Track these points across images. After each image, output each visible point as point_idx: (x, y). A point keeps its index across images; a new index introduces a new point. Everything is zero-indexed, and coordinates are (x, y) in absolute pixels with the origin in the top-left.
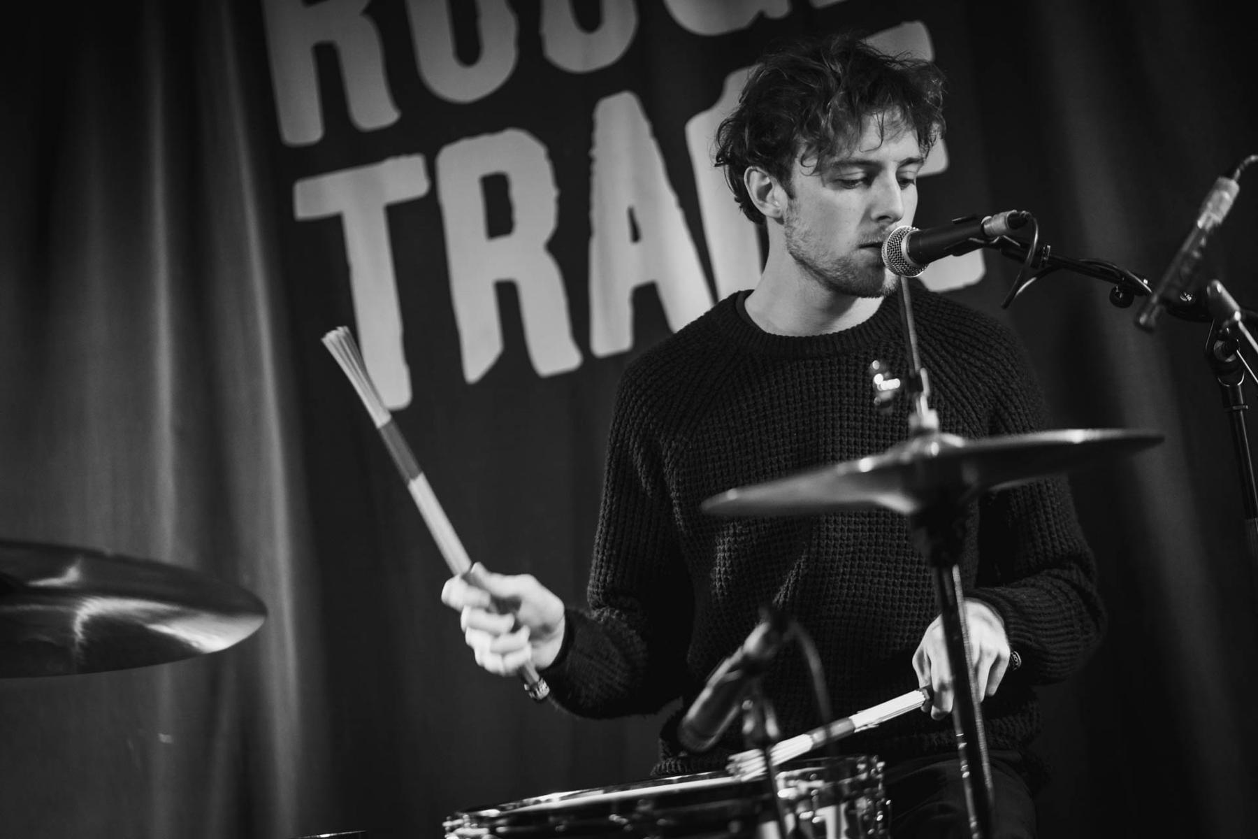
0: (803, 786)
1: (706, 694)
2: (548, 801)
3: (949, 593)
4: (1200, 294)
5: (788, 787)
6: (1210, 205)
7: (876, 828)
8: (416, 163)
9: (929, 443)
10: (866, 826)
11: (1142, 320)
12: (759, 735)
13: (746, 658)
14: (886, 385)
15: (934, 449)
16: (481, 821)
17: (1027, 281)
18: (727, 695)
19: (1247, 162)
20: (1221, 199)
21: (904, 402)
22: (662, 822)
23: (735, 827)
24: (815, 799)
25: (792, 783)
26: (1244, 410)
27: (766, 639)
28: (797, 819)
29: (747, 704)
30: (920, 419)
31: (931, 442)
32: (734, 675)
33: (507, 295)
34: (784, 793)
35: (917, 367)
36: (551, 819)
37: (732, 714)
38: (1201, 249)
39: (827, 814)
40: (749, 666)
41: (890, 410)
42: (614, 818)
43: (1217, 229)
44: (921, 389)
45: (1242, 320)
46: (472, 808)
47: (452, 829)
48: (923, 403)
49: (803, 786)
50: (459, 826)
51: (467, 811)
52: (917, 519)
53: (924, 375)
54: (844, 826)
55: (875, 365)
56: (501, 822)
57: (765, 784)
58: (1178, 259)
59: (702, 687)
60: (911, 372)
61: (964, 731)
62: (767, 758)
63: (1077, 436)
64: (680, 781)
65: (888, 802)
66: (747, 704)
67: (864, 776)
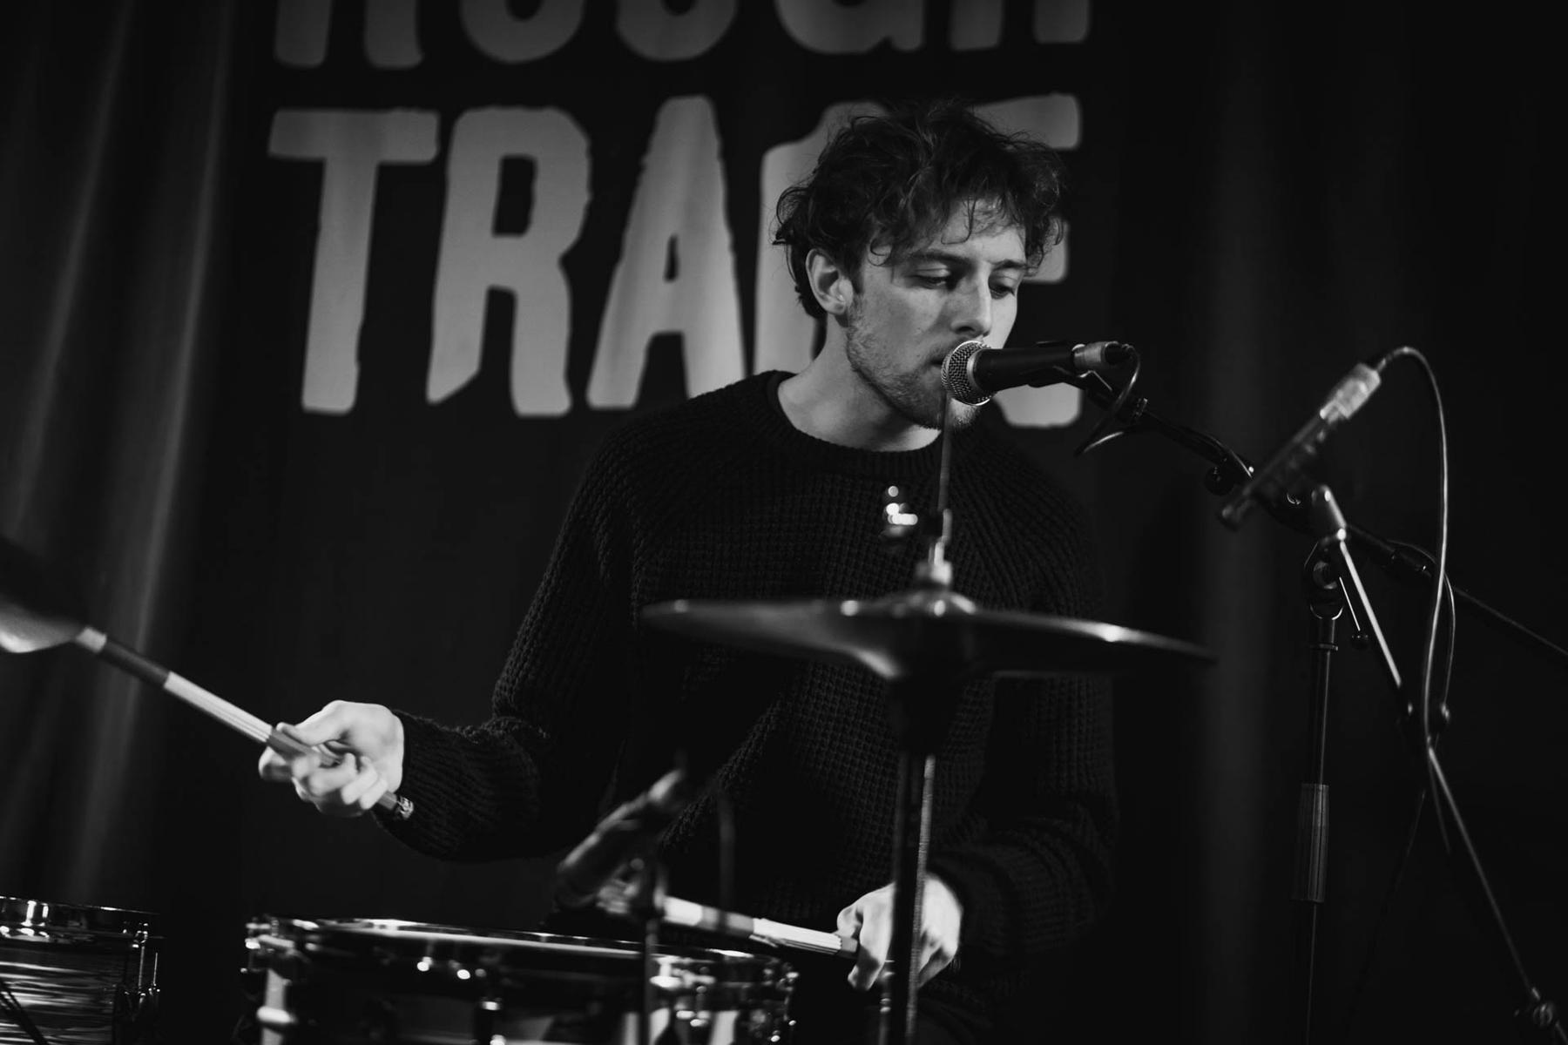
0: (690, 978)
1: (592, 840)
2: (383, 927)
3: (915, 790)
5: (673, 976)
6: (1340, 394)
8: (428, 123)
11: (1226, 512)
14: (899, 517)
15: (939, 608)
16: (288, 931)
17: (1110, 434)
19: (1397, 352)
20: (1355, 391)
21: (916, 543)
22: (507, 982)
24: (700, 998)
25: (677, 971)
26: (1333, 651)
27: (676, 792)
28: (673, 1017)
29: (637, 863)
30: (930, 569)
31: (938, 599)
32: (629, 825)
33: (501, 308)
34: (665, 979)
35: (941, 505)
38: (1317, 444)
40: (651, 817)
43: (1342, 423)
44: (939, 533)
45: (1346, 541)
46: (284, 916)
47: (256, 934)
48: (938, 551)
49: (690, 978)
51: (278, 916)
53: (947, 518)
55: (892, 491)
56: (313, 937)
64: (550, 940)
65: (792, 1023)
66: (637, 863)
67: (768, 983)
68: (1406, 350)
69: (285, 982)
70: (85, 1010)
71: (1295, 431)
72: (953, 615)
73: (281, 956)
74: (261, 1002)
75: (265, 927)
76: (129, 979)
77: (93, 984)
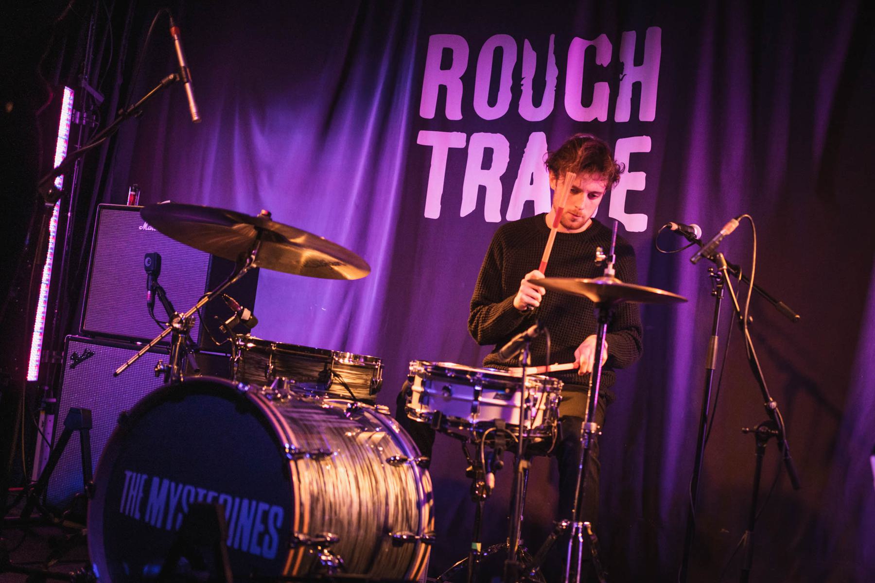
0: (534, 383)
1: (510, 344)
3: (601, 333)
4: (715, 256)
5: (529, 382)
7: (554, 404)
9: (608, 280)
10: (551, 402)
12: (524, 362)
13: (527, 335)
14: (600, 256)
15: (610, 282)
16: (423, 365)
18: (517, 346)
20: (731, 226)
21: (604, 264)
22: (483, 382)
23: (507, 391)
24: (537, 389)
25: (531, 381)
27: (535, 330)
28: (529, 394)
29: (523, 351)
36: (447, 371)
37: (518, 352)
38: (719, 241)
39: (539, 395)
40: (527, 338)
41: (599, 265)
42: (468, 376)
44: (611, 261)
47: (412, 365)
50: (415, 365)
51: (419, 361)
52: (597, 304)
54: (544, 400)
55: (599, 248)
56: (429, 367)
57: (520, 380)
58: (712, 242)
59: (510, 340)
60: (610, 255)
61: (593, 381)
62: (524, 370)
63: (659, 292)
64: (494, 371)
66: (523, 351)
68: (746, 215)
69: (421, 379)
70: (363, 384)
71: (713, 238)
72: (614, 286)
73: (420, 372)
74: (413, 384)
75: (414, 363)
76: (374, 376)
77: (365, 377)
